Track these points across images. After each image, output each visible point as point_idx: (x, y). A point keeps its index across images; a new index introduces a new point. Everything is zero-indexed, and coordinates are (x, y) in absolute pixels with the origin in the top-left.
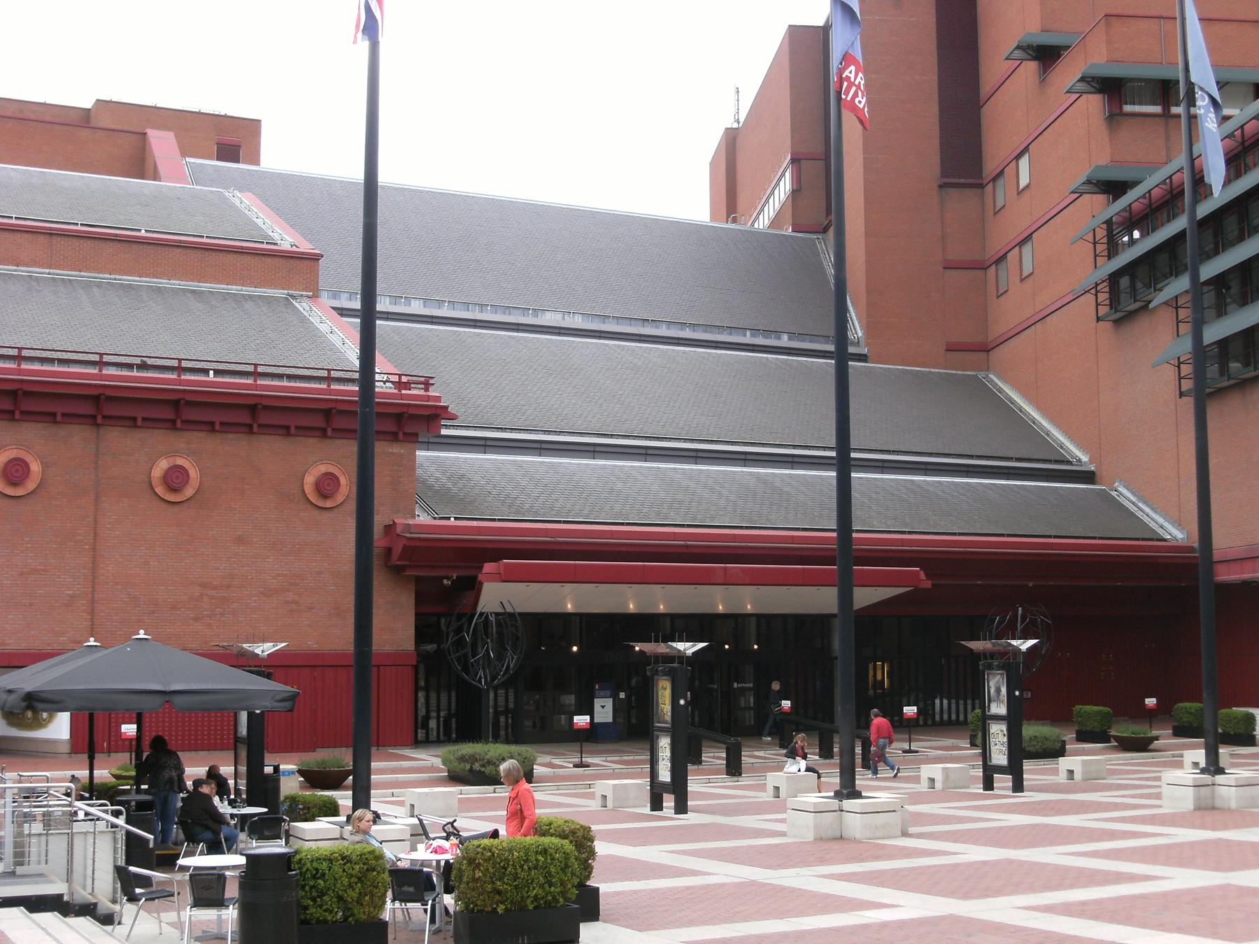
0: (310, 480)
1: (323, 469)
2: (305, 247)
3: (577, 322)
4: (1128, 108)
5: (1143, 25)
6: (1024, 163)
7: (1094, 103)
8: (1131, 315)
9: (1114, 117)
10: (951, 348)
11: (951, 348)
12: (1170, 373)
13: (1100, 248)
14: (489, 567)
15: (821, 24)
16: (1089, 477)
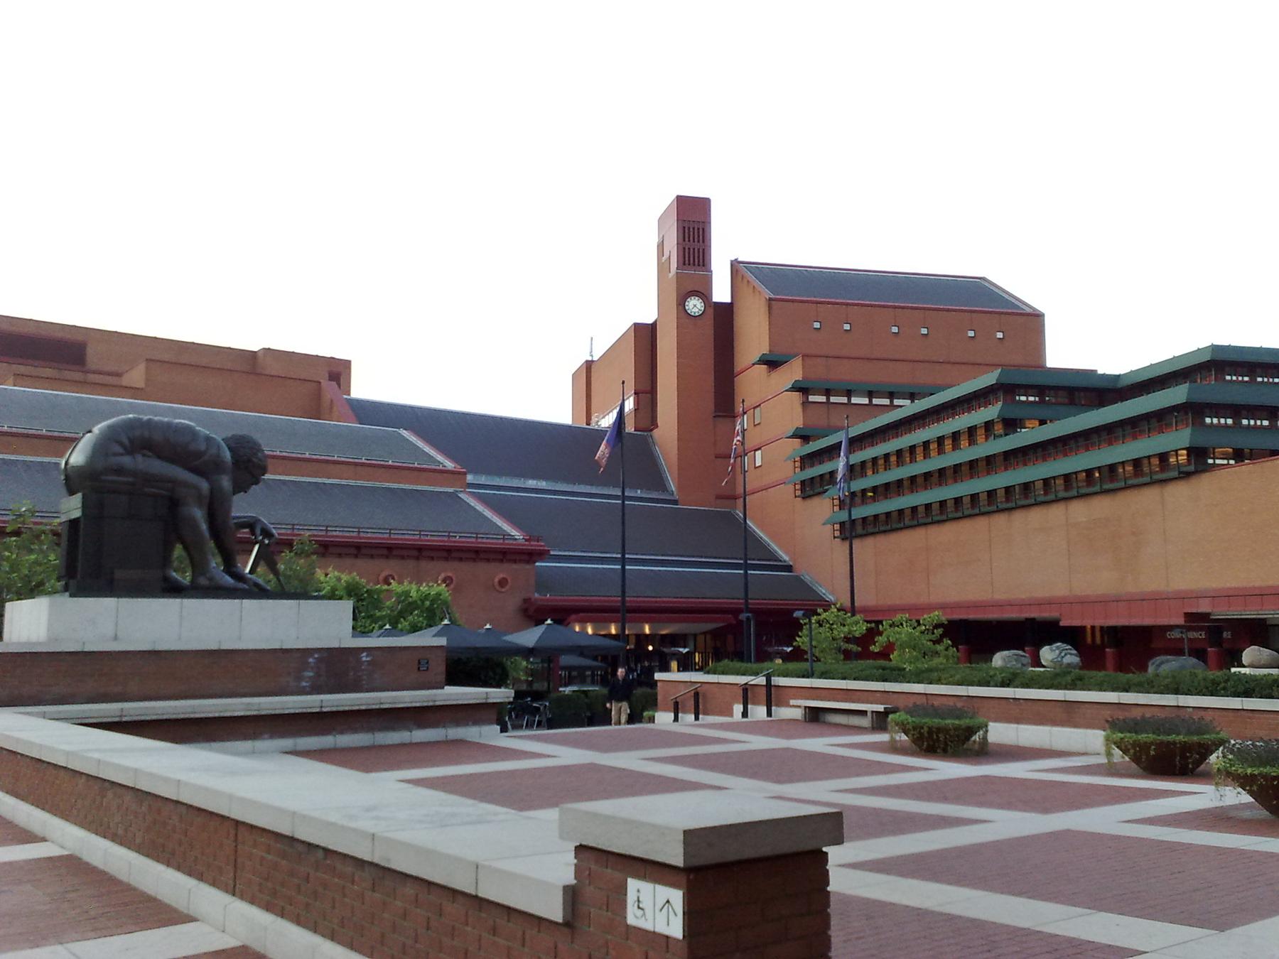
0: (496, 580)
1: (502, 576)
2: (459, 468)
3: (543, 484)
4: (812, 398)
5: (819, 360)
6: (757, 410)
7: (796, 396)
8: (810, 496)
9: (806, 404)
10: (718, 497)
11: (718, 497)
12: (829, 527)
13: (798, 464)
14: (573, 616)
15: (650, 321)
16: (789, 568)
